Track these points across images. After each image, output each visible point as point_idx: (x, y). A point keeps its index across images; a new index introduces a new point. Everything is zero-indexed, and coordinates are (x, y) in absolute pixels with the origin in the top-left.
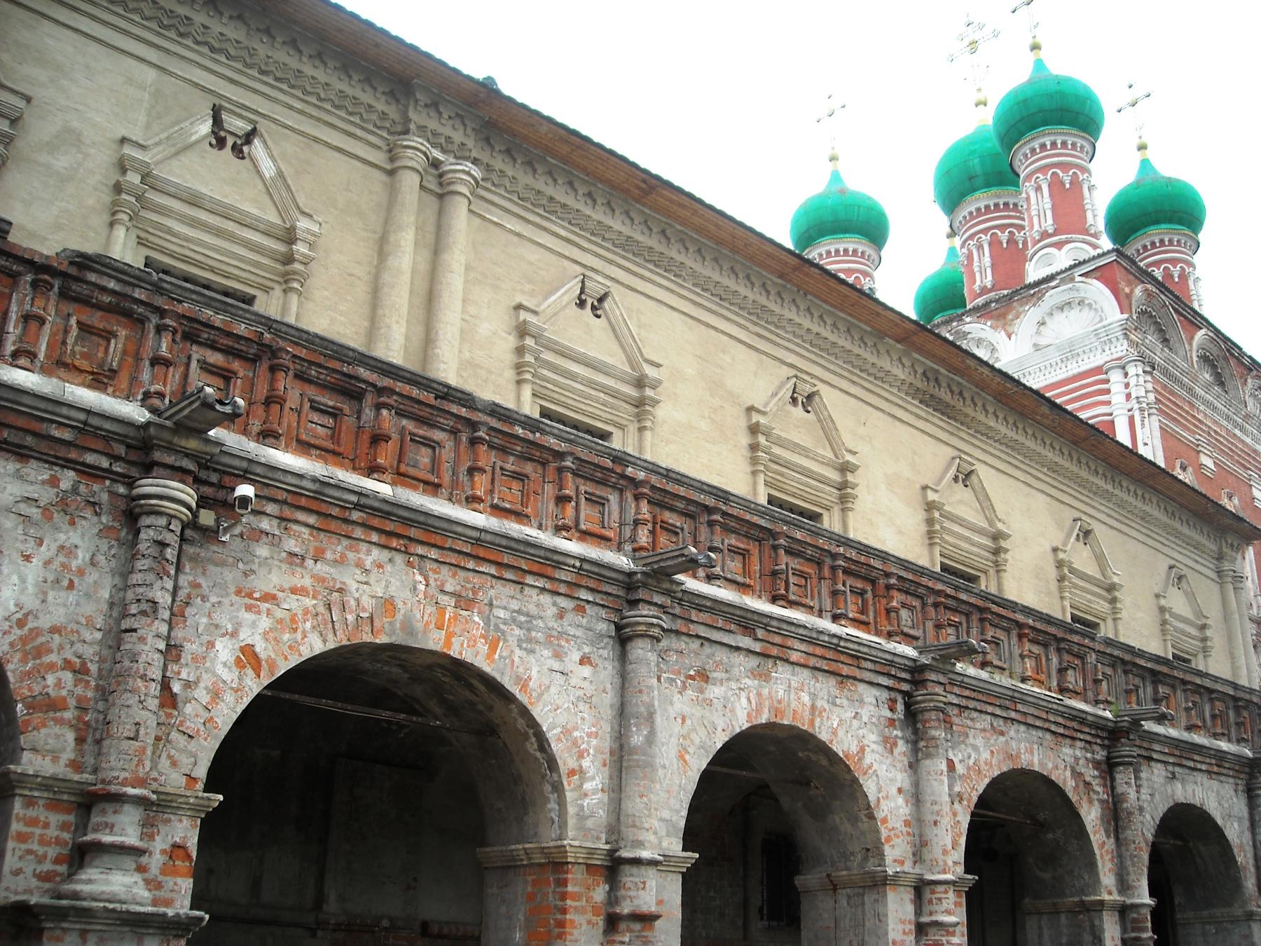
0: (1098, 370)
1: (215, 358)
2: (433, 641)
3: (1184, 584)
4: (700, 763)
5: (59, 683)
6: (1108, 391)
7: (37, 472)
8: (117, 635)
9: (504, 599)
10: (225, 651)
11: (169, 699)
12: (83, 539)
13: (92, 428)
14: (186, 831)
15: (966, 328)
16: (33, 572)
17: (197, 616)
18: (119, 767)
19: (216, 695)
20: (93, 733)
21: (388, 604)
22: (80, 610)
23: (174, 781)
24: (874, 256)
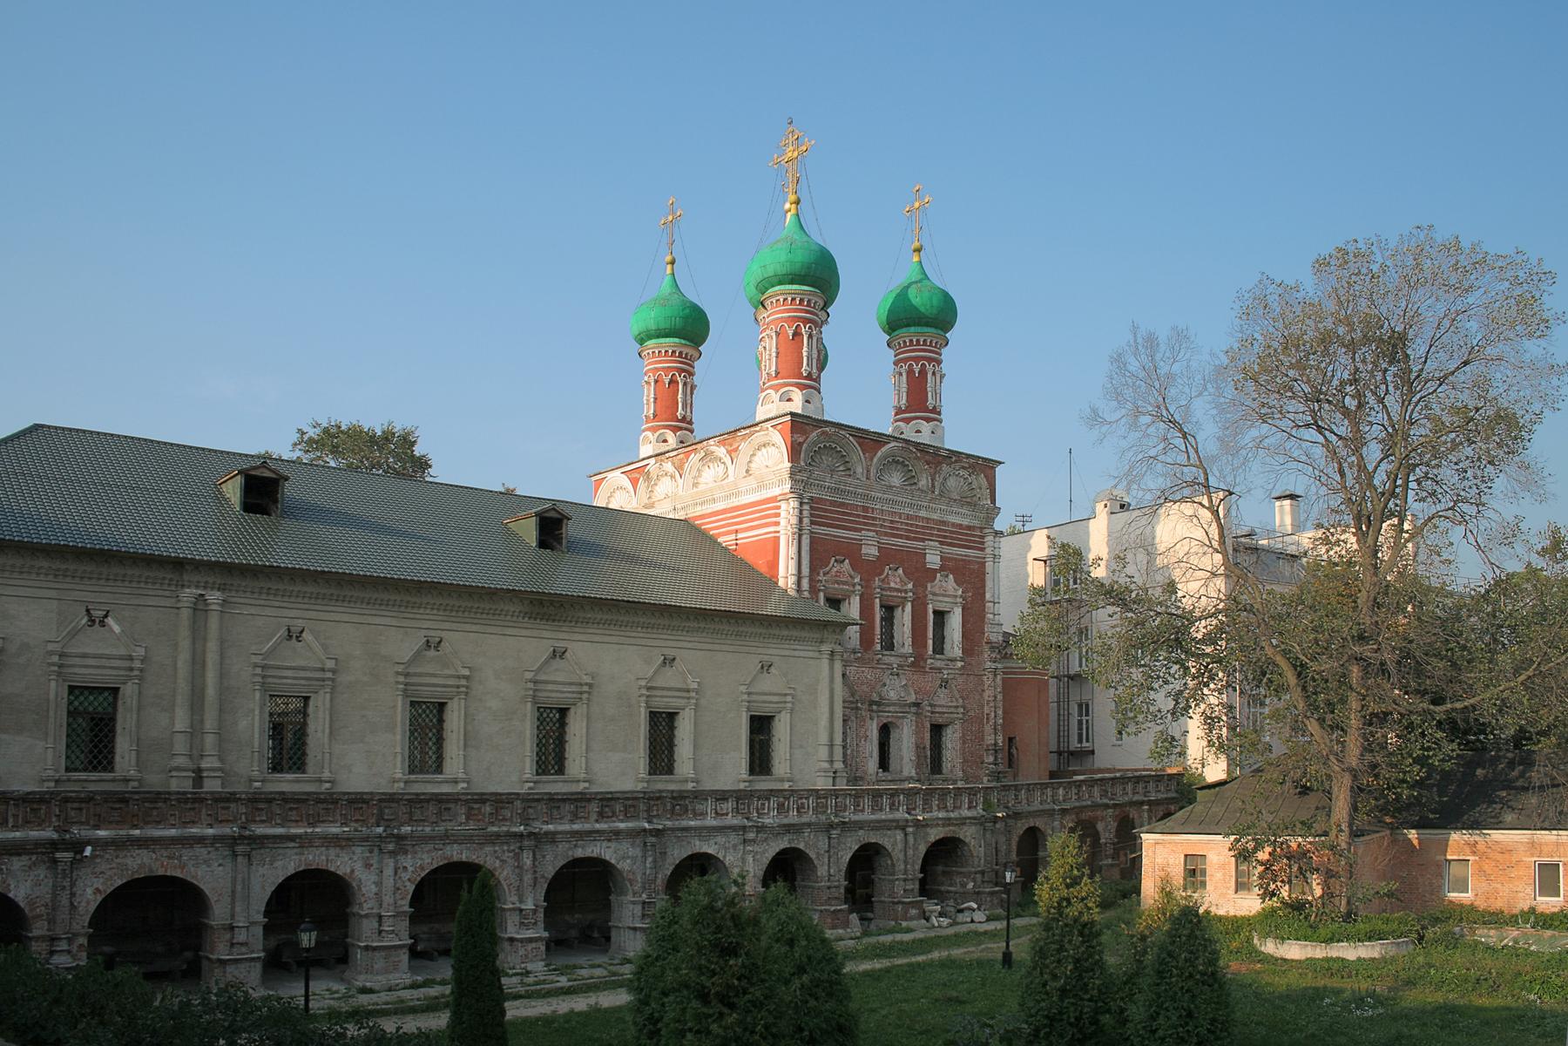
0: (774, 499)
1: (76, 805)
2: (161, 872)
3: (772, 670)
4: (270, 889)
5: (40, 910)
6: (778, 515)
7: (24, 858)
8: (55, 896)
9: (186, 854)
10: (89, 891)
11: (73, 906)
12: (42, 872)
13: (38, 844)
14: (83, 941)
15: (713, 448)
16: (28, 884)
17: (80, 884)
18: (59, 931)
19: (88, 903)
20: (52, 921)
21: (142, 866)
22: (45, 891)
23: (76, 927)
24: (696, 354)
